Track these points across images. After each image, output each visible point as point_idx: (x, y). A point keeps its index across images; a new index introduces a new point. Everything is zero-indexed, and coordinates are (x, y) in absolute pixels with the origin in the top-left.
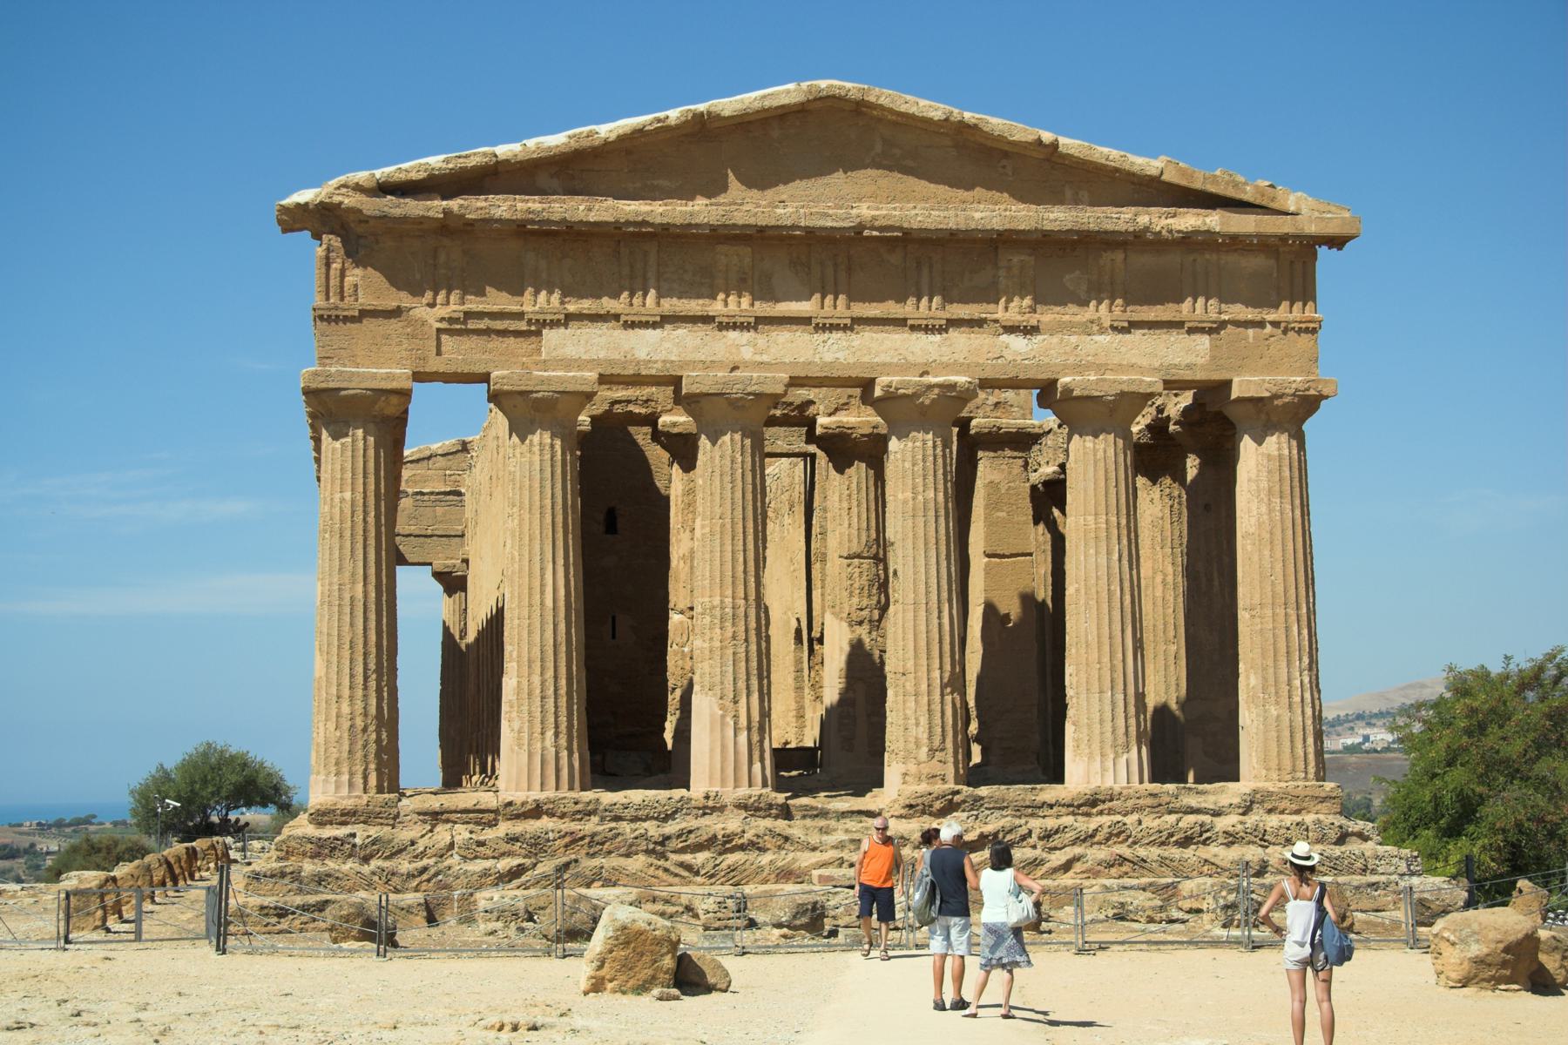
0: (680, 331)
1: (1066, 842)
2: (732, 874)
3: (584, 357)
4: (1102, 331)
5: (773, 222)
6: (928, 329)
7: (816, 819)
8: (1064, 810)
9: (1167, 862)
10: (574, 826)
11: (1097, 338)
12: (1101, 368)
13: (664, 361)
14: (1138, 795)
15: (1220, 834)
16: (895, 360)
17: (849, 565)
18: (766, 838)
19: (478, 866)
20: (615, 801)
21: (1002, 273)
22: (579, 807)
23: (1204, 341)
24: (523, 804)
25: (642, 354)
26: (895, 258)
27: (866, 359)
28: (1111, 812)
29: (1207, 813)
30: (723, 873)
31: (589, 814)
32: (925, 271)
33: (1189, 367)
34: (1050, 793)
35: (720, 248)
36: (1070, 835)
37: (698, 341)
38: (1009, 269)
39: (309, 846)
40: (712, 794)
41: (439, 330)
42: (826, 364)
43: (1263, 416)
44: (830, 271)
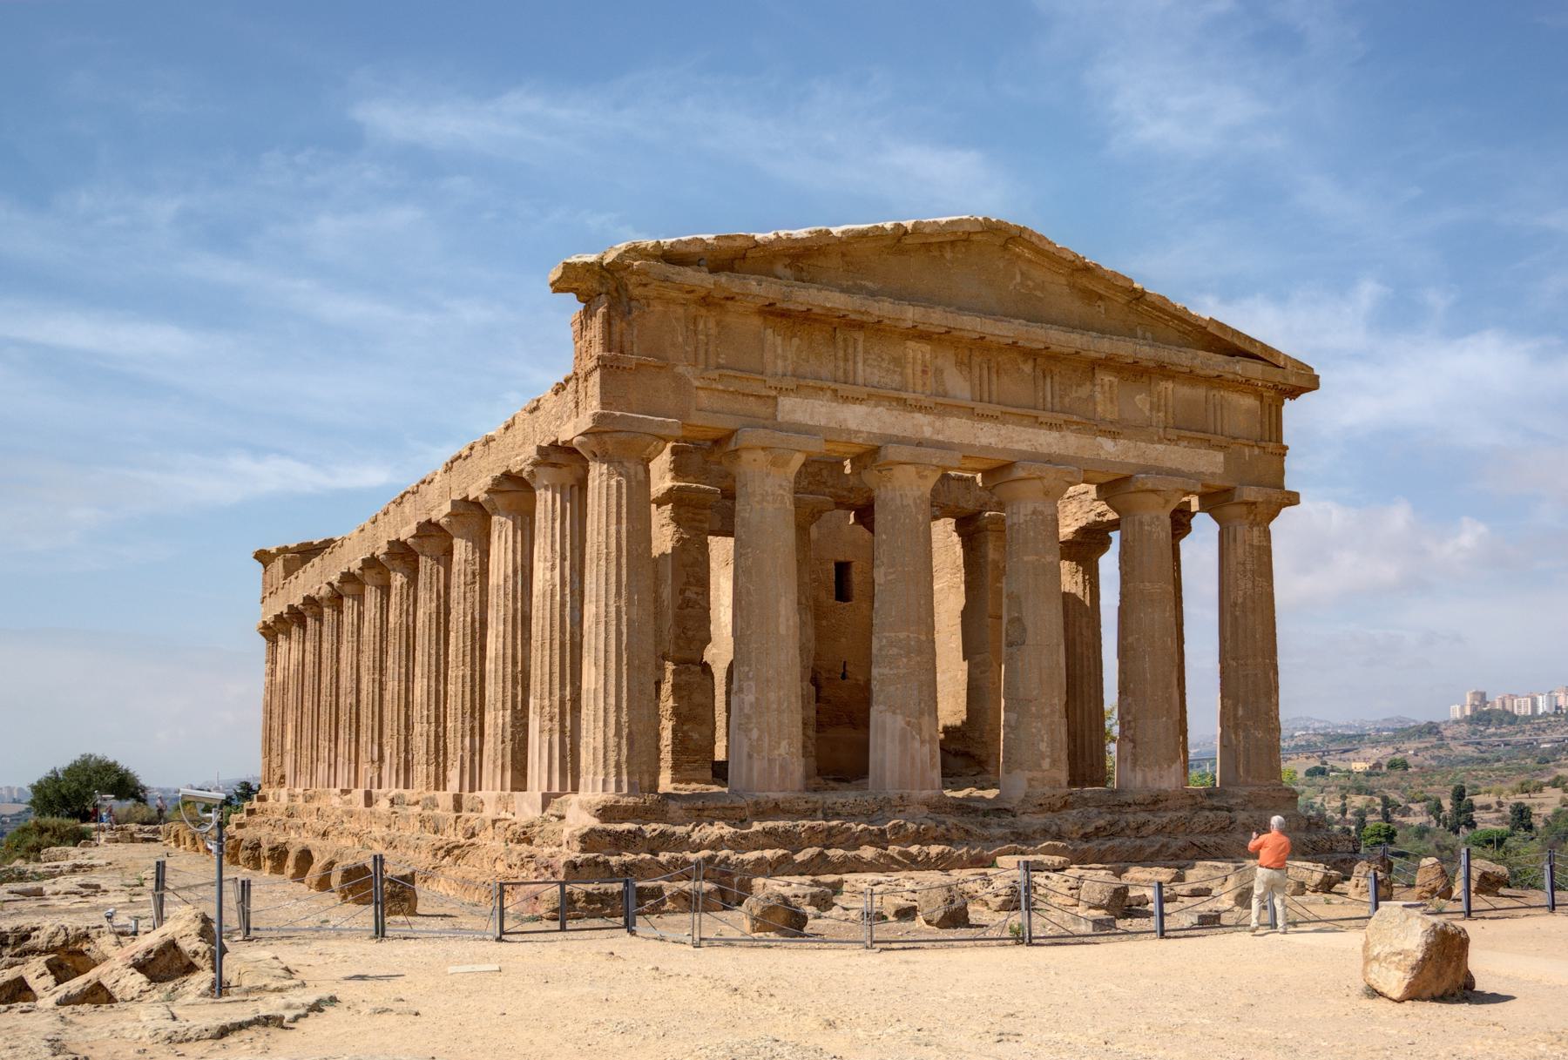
0: (880, 409)
3: (810, 423)
4: (1160, 441)
5: (958, 327)
6: (1051, 426)
11: (1158, 446)
12: (1159, 471)
13: (869, 433)
16: (1029, 449)
19: (752, 855)
21: (1098, 388)
22: (810, 805)
23: (1220, 457)
24: (766, 803)
25: (853, 425)
26: (1027, 368)
27: (1009, 446)
32: (1048, 381)
33: (1213, 474)
35: (910, 344)
37: (893, 419)
38: (1102, 386)
39: (608, 838)
40: (905, 795)
41: (697, 388)
42: (983, 448)
43: (1252, 517)
44: (985, 372)
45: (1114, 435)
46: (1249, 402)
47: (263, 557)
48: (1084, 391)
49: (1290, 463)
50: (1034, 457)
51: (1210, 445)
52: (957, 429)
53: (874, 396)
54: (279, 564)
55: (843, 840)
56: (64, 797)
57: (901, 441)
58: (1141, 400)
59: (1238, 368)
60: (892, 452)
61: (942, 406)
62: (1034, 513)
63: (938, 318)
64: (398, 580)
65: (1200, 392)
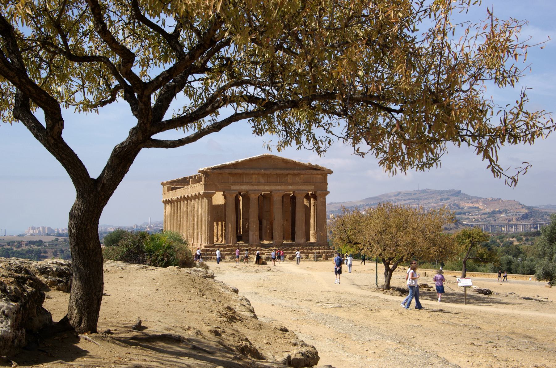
6: (279, 185)
12: (300, 190)
23: (313, 186)
25: (244, 189)
26: (275, 176)
45: (291, 185)
46: (320, 176)
47: (163, 184)
48: (286, 178)
49: (328, 186)
50: (276, 190)
51: (311, 185)
52: (261, 187)
53: (247, 184)
54: (166, 187)
56: (113, 240)
57: (251, 190)
58: (297, 179)
59: (315, 172)
60: (249, 192)
61: (259, 184)
63: (256, 172)
64: (186, 202)
65: (310, 176)
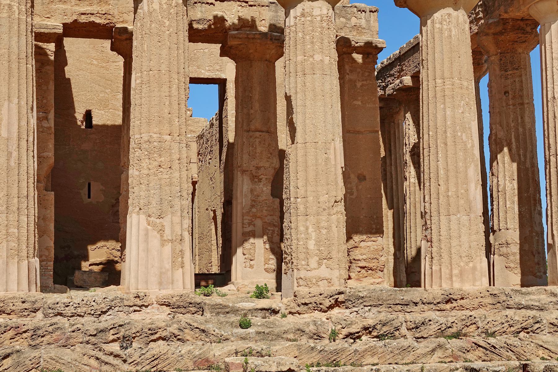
1: (431, 332)
2: (156, 362)
7: (228, 315)
8: (426, 307)
9: (513, 348)
10: (21, 321)
14: (482, 295)
15: (547, 325)
17: (251, 137)
18: (186, 331)
20: (58, 300)
22: (25, 305)
28: (462, 308)
29: (533, 309)
30: (148, 362)
31: (35, 311)
34: (414, 294)
36: (433, 328)
55: (51, 341)
62: (303, 15)
